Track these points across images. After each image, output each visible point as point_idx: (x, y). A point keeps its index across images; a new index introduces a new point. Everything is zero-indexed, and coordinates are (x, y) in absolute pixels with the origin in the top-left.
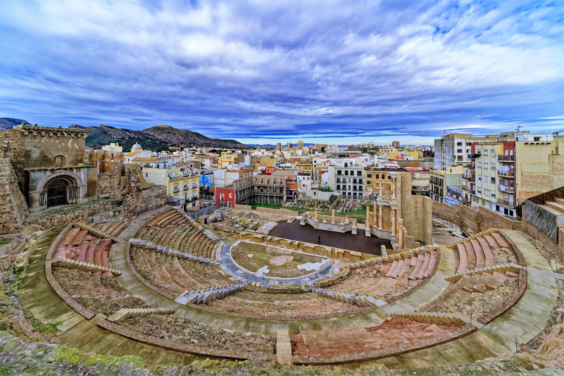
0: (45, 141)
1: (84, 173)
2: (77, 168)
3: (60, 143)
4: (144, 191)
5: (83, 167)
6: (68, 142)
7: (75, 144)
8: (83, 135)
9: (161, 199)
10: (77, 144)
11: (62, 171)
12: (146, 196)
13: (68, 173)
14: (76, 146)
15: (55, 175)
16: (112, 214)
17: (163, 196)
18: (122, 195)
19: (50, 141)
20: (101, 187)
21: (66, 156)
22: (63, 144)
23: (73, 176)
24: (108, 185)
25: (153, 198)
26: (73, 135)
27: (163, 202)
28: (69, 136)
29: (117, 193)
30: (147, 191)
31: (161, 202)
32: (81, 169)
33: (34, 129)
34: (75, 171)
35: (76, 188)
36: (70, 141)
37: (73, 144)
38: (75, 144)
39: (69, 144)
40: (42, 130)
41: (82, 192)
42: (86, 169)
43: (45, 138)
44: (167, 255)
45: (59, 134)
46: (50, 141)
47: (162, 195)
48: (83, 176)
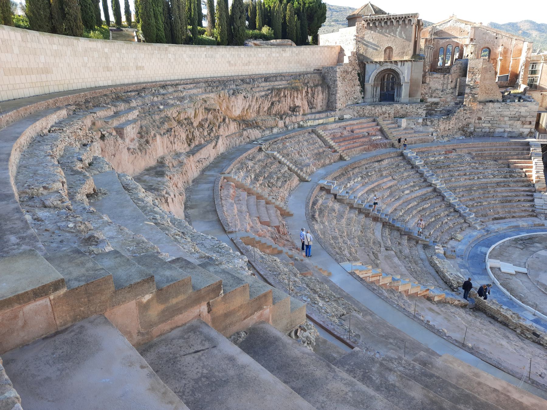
1: (408, 68)
2: (401, 61)
4: (491, 104)
5: (406, 61)
6: (396, 31)
8: (410, 20)
9: (523, 123)
10: (404, 33)
11: (389, 64)
12: (494, 113)
13: (394, 67)
15: (382, 69)
16: (420, 121)
17: (528, 119)
18: (456, 104)
20: (430, 88)
21: (394, 48)
23: (397, 70)
24: (440, 87)
25: (506, 119)
26: (401, 22)
28: (398, 23)
29: (449, 100)
30: (496, 105)
31: (522, 130)
32: (406, 63)
34: (399, 64)
35: (400, 85)
36: (398, 30)
41: (405, 91)
42: (410, 63)
43: (378, 29)
44: (425, 181)
45: (389, 23)
47: (526, 117)
48: (406, 72)
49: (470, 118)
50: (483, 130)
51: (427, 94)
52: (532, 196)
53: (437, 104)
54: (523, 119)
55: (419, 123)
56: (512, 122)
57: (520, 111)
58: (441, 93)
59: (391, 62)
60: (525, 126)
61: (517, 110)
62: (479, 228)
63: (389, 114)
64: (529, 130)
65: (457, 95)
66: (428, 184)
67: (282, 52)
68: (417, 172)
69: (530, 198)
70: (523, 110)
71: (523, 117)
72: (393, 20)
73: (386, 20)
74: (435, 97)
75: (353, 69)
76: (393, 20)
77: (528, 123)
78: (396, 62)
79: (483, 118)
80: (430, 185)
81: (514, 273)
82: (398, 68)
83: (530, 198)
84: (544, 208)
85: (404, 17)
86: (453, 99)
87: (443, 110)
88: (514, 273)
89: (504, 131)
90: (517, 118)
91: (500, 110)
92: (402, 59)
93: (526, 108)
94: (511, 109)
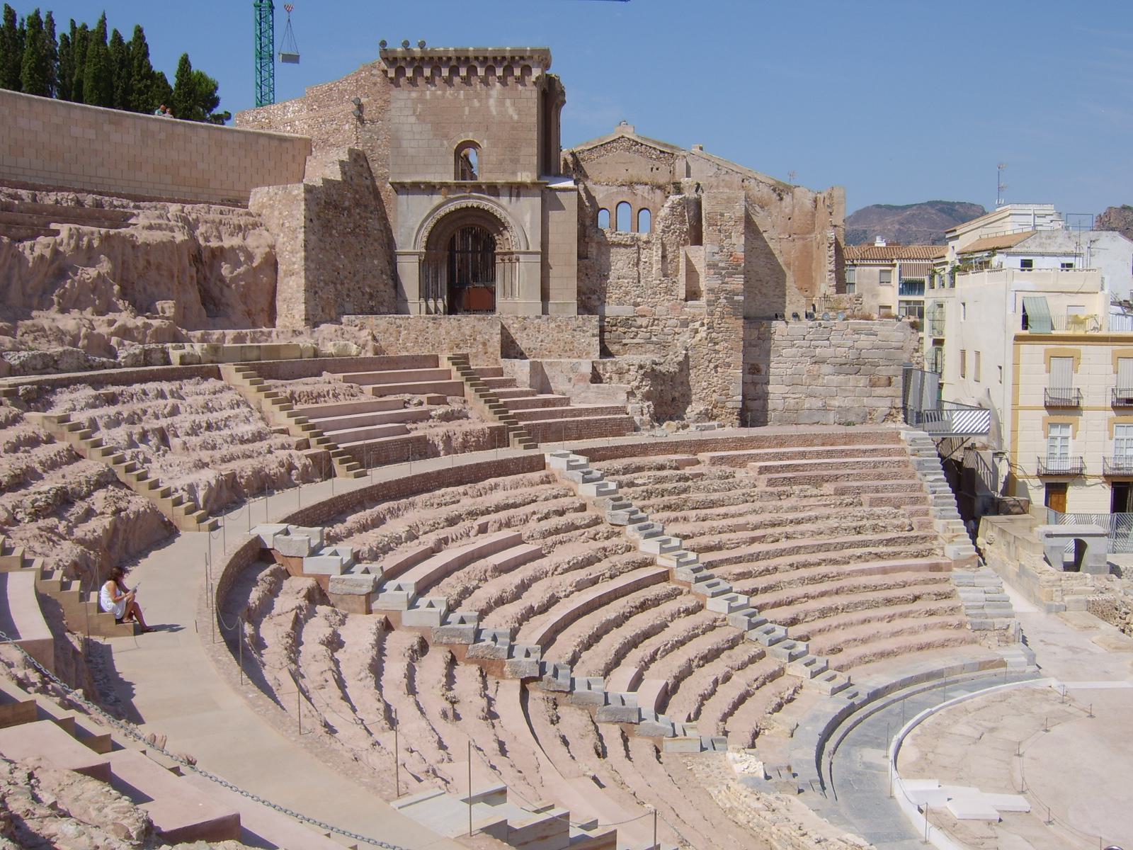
0: (433, 93)
3: (468, 99)
6: (488, 96)
7: (508, 102)
10: (514, 104)
13: (487, 203)
14: (511, 111)
16: (586, 369)
17: (884, 372)
19: (443, 96)
22: (476, 103)
23: (499, 213)
27: (883, 406)
33: (405, 59)
37: (501, 102)
38: (508, 102)
39: (492, 102)
40: (422, 59)
46: (443, 96)
48: (527, 218)
51: (594, 292)
55: (583, 376)
56: (841, 377)
59: (478, 188)
60: (879, 391)
61: (850, 343)
63: (484, 344)
64: (888, 403)
65: (683, 296)
67: (106, 128)
70: (864, 341)
72: (476, 63)
73: (453, 63)
75: (358, 204)
76: (476, 63)
77: (884, 381)
78: (493, 190)
82: (502, 207)
85: (508, 55)
86: (673, 308)
89: (825, 409)
91: (806, 343)
92: (511, 179)
94: (835, 339)
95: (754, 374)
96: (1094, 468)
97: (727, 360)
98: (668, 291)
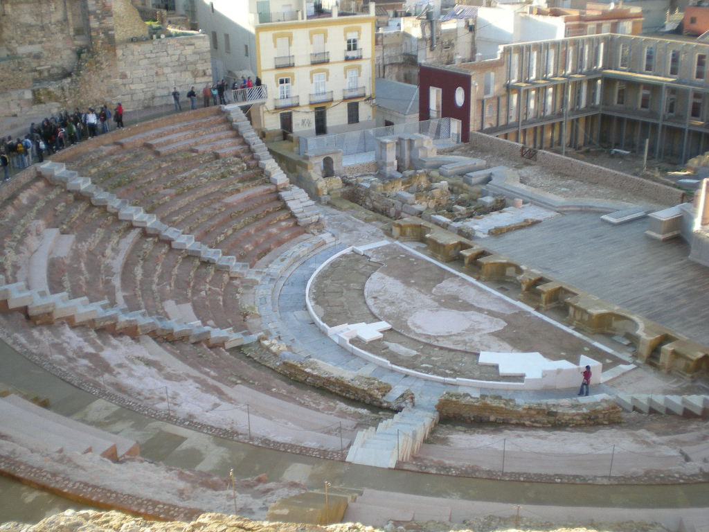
16: (28, 95)
17: (200, 67)
47: (194, 63)
49: (110, 76)
50: (135, 98)
51: (13, 39)
52: (279, 199)
53: (37, 57)
54: (190, 67)
57: (184, 52)
58: (41, 34)
60: (199, 80)
62: (258, 279)
66: (124, 225)
68: (92, 206)
69: (279, 205)
71: (191, 63)
74: (31, 43)
79: (129, 75)
80: (131, 226)
81: (381, 335)
83: (279, 205)
84: (308, 214)
87: (52, 67)
88: (381, 335)
90: (183, 65)
91: (154, 55)
93: (193, 47)
95: (122, 79)
96: (304, 101)
97: (109, 74)
98: (62, 31)
